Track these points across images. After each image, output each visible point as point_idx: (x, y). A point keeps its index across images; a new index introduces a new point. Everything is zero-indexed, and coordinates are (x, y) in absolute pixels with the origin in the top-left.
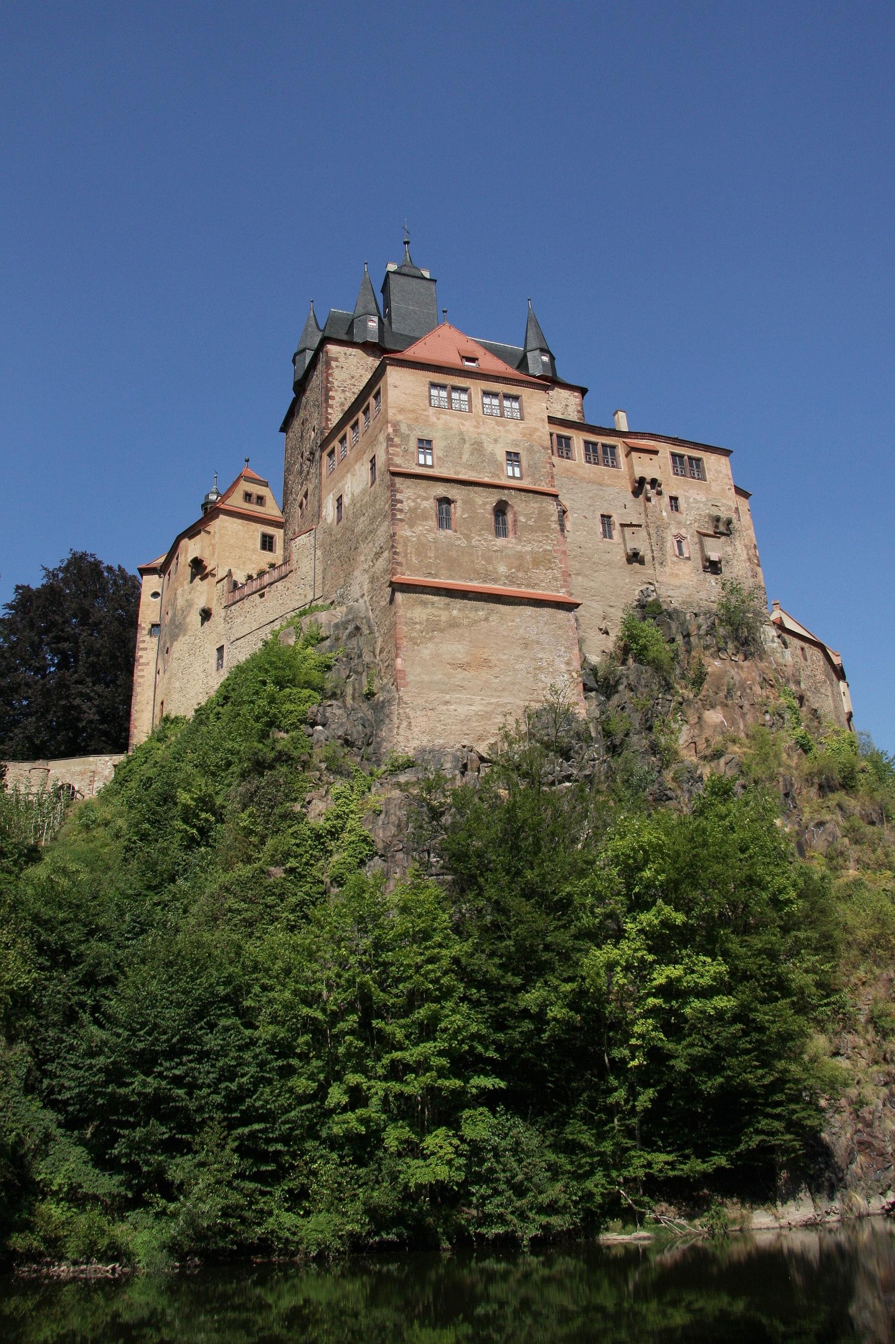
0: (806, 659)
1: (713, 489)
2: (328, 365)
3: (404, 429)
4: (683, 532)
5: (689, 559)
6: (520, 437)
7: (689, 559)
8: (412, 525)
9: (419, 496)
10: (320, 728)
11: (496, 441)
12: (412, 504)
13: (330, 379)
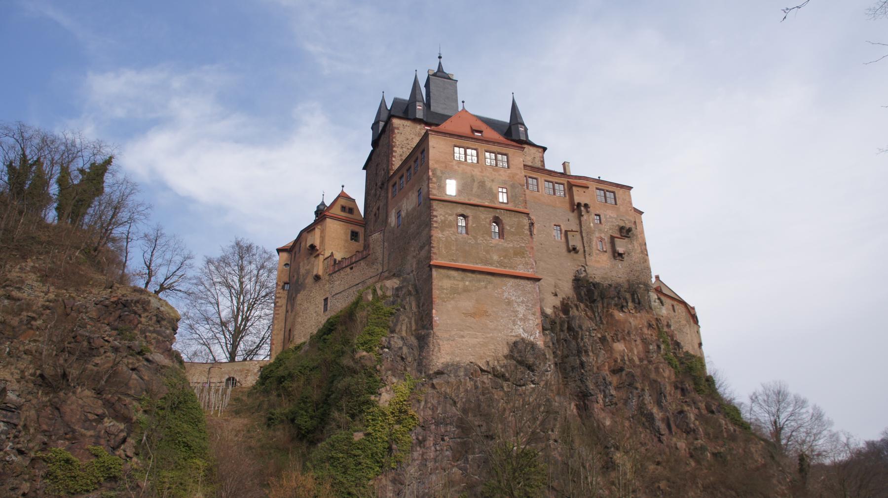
0: (674, 311)
1: (621, 210)
2: (393, 132)
3: (439, 173)
4: (603, 235)
5: (606, 252)
6: (507, 179)
7: (606, 252)
8: (442, 231)
9: (447, 213)
10: (386, 350)
11: (493, 181)
12: (443, 218)
13: (394, 140)
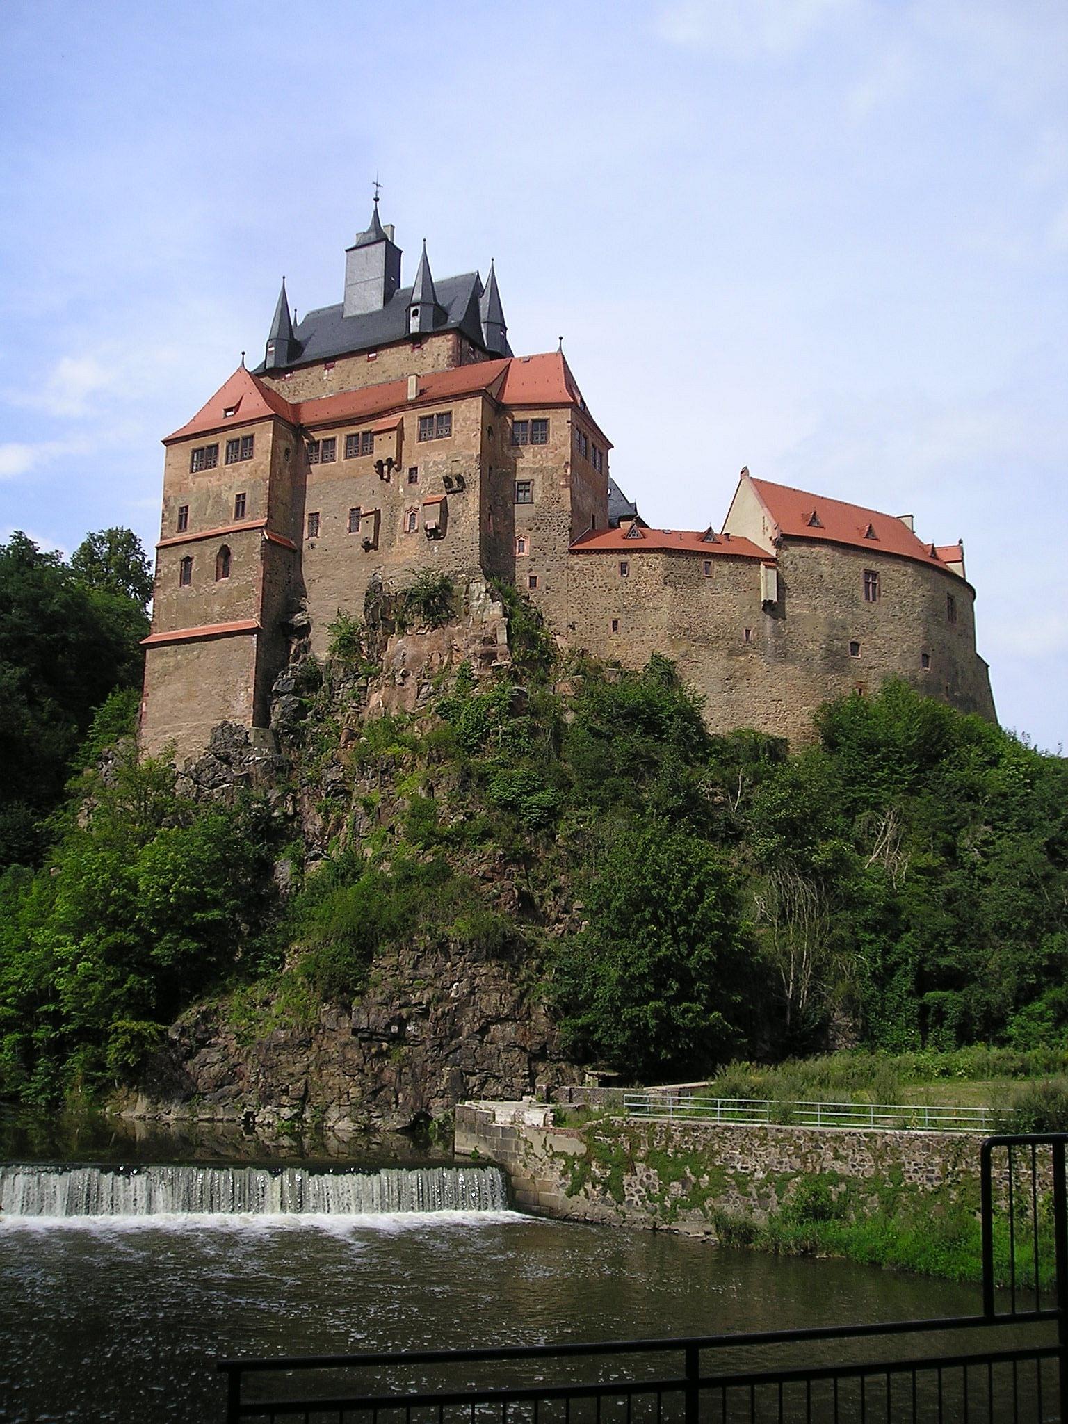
7: (417, 531)
